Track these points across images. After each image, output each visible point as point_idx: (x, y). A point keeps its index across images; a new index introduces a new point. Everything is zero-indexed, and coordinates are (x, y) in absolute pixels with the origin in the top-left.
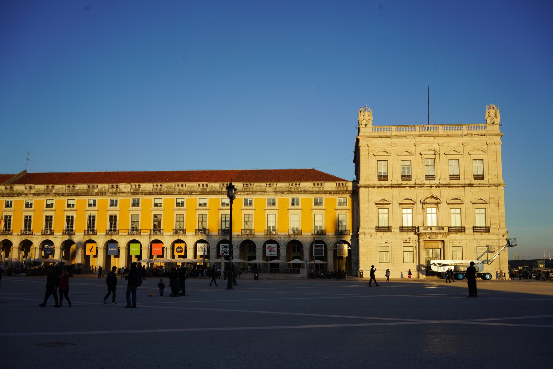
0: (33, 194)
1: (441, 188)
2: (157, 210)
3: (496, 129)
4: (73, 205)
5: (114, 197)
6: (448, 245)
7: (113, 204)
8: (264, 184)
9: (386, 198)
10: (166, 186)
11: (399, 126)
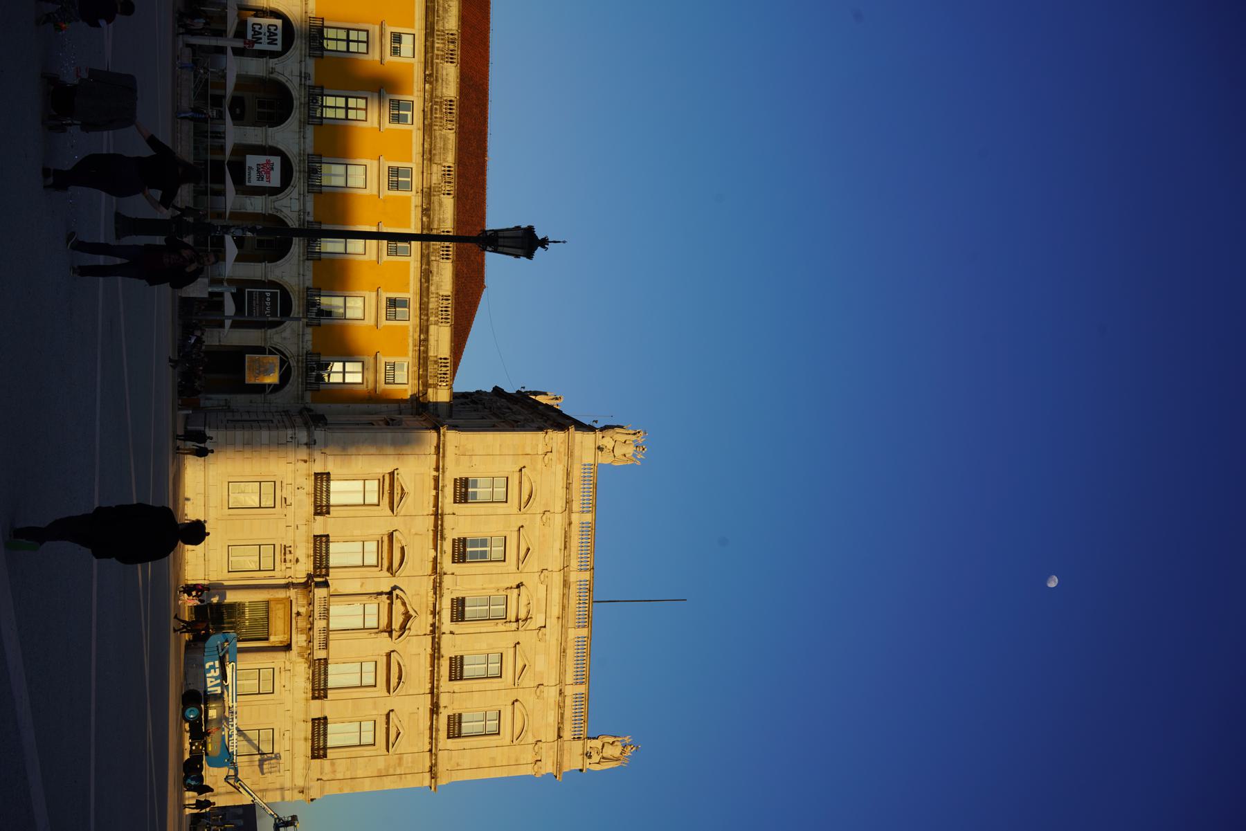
1: (429, 638)
3: (574, 761)
6: (279, 659)
8: (450, 159)
9: (408, 500)
11: (592, 530)
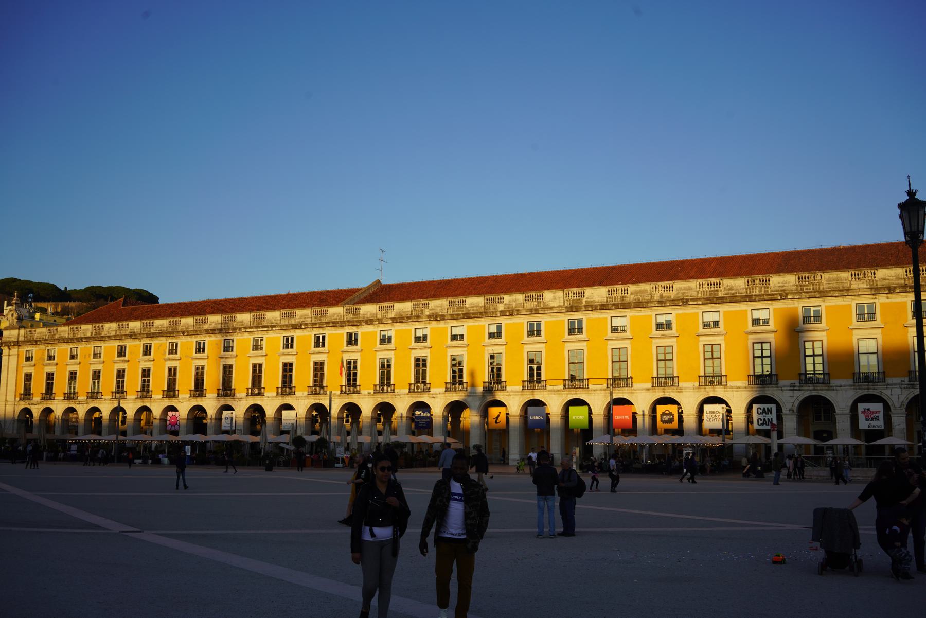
0: (392, 319)
2: (617, 339)
4: (462, 336)
5: (534, 318)
7: (535, 331)
8: (845, 275)
10: (634, 290)
